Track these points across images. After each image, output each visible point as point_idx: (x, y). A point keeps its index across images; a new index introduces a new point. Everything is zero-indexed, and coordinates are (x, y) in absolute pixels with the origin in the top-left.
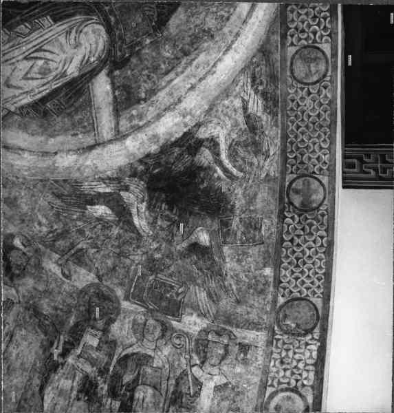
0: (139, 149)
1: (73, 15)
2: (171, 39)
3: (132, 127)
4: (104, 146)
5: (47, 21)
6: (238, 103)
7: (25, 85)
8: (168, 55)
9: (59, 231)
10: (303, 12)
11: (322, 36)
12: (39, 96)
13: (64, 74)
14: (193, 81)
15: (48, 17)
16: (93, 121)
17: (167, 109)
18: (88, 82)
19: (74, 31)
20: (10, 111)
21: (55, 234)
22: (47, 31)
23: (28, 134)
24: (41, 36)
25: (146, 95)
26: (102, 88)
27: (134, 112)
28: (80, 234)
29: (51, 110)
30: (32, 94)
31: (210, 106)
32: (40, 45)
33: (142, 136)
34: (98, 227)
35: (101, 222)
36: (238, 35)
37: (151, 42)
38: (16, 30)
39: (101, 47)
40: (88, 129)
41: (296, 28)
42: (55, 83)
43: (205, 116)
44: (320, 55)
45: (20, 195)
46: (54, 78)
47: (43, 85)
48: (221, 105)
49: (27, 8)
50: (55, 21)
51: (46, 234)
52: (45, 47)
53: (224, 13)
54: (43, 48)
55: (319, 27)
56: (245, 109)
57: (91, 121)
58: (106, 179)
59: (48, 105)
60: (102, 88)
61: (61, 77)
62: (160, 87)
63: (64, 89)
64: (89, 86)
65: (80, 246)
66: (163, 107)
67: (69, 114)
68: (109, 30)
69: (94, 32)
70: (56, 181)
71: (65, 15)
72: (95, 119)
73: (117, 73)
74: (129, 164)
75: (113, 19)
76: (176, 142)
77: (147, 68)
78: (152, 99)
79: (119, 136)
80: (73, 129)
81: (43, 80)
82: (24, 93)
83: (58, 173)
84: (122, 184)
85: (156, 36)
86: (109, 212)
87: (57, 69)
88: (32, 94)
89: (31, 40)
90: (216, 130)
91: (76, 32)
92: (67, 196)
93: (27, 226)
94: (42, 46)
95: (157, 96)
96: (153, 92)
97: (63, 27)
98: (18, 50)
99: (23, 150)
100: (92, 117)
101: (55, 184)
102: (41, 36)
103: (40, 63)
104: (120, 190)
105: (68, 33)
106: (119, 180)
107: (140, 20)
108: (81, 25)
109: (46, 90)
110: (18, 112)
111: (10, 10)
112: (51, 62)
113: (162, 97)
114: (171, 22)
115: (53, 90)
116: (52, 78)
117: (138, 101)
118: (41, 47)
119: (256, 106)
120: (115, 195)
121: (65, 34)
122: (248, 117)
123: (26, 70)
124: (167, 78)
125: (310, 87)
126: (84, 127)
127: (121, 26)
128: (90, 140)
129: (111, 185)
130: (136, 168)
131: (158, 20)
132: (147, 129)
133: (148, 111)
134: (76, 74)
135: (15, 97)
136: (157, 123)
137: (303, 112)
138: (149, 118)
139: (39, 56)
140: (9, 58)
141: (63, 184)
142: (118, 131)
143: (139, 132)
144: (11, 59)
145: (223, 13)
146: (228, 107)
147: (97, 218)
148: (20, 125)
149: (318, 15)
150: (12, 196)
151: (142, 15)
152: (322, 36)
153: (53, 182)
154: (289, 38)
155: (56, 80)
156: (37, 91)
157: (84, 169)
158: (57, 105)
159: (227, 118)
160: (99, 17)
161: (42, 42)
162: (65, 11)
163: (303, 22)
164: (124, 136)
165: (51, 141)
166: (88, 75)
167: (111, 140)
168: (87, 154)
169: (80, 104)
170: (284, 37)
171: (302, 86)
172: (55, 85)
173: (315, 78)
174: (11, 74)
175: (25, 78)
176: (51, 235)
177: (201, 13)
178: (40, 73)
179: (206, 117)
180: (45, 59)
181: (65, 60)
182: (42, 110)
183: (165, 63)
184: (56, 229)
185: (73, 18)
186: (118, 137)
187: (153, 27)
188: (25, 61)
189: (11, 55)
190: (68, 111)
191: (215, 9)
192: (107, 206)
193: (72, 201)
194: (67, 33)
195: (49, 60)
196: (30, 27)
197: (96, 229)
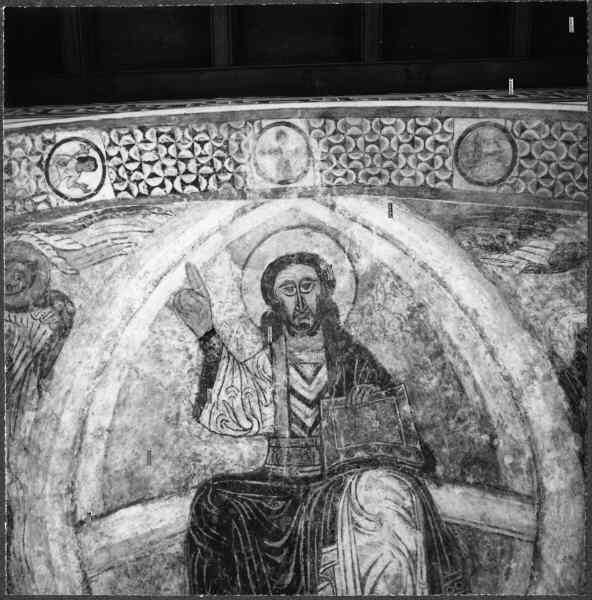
1: (334, 514)
2: (412, 372)
3: (530, 472)
4: (544, 532)
5: (328, 554)
6: (528, 280)
8: (435, 381)
10: (403, 160)
11: (443, 133)
13: (412, 557)
14: (482, 349)
15: (324, 550)
16: (498, 534)
17: (516, 401)
18: (439, 522)
19: (359, 519)
22: (341, 559)
24: (345, 571)
25: (486, 432)
26: (454, 502)
27: (508, 460)
31: (525, 329)
33: (548, 459)
36: (424, 266)
37: (410, 404)
39: (394, 484)
40: (508, 549)
41: (426, 172)
42: (419, 575)
43: (540, 340)
44: (471, 137)
46: (411, 574)
48: (527, 309)
49: (299, 580)
50: (333, 542)
52: (363, 571)
53: (389, 283)
54: (363, 575)
55: (429, 136)
56: (539, 270)
57: (498, 538)
60: (454, 502)
61: (414, 562)
62: (481, 407)
63: (434, 563)
64: (446, 523)
66: (511, 409)
67: (475, 571)
68: (373, 463)
69: (368, 488)
71: (331, 524)
72: (496, 531)
73: (439, 470)
75: (359, 454)
76: (572, 402)
77: (447, 419)
79: (536, 498)
80: (498, 573)
85: (401, 394)
87: (400, 565)
89: (344, 588)
90: (567, 325)
91: (361, 515)
95: (491, 413)
96: (484, 420)
97: (346, 533)
100: (494, 533)
102: (345, 571)
105: (357, 527)
107: (373, 413)
108: (353, 505)
112: (387, 570)
113: (496, 406)
114: (387, 367)
115: (428, 581)
116: (409, 577)
117: (493, 448)
118: (360, 578)
119: (538, 250)
121: (357, 534)
122: (555, 267)
124: (469, 390)
125: (519, 154)
126: (503, 552)
127: (373, 445)
128: (526, 551)
131: (381, 386)
132: (540, 447)
133: (511, 436)
134: (420, 537)
136: (534, 426)
137: (560, 170)
138: (523, 437)
139: (371, 586)
142: (529, 497)
143: (541, 462)
145: (387, 285)
146: (532, 298)
149: (411, 137)
151: (367, 408)
152: (443, 133)
154: (438, 185)
155: (416, 573)
157: (565, 580)
158: (453, 584)
159: (551, 303)
160: (351, 474)
161: (354, 571)
162: (326, 522)
163: (418, 162)
164: (539, 490)
166: (429, 518)
167: (538, 514)
168: (544, 567)
169: (466, 546)
170: (437, 194)
171: (516, 168)
172: (422, 578)
173: (507, 146)
177: (383, 317)
179: (543, 339)
180: (379, 577)
181: (393, 546)
183: (446, 389)
185: (340, 513)
190: (469, 571)
191: (380, 296)
195: (383, 572)
196: (326, 583)
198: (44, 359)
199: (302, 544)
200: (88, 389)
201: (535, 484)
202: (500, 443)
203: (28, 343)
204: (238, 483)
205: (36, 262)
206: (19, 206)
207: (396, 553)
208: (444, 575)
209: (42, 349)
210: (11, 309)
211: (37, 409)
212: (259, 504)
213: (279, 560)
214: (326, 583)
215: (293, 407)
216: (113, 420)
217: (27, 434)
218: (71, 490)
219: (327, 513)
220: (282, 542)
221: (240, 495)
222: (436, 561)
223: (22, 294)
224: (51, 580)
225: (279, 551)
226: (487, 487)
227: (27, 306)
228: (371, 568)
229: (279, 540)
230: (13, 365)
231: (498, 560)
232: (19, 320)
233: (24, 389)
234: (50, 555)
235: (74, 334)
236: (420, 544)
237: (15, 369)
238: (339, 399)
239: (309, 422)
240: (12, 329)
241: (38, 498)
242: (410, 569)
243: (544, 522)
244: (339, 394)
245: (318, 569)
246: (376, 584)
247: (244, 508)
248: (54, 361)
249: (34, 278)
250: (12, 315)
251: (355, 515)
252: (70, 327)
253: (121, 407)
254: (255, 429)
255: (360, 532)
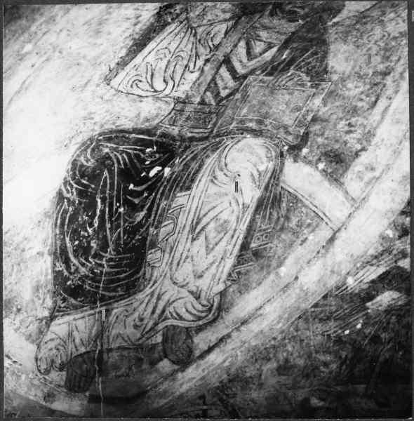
0: (393, 200)
3: (369, 183)
5: (181, 198)
7: (214, 256)
9: (350, 356)
12: (238, 247)
16: (314, 212)
20: (221, 293)
21: (348, 362)
23: (255, 288)
24: (189, 213)
25: (361, 144)
28: (376, 343)
29: (261, 245)
30: (228, 255)
32: (197, 216)
34: (392, 321)
35: (394, 312)
38: (160, 240)
40: (314, 224)
45: (288, 352)
46: (237, 222)
47: (233, 237)
49: (150, 217)
50: (189, 188)
51: (338, 370)
52: (203, 213)
57: (313, 214)
58: (373, 260)
59: (253, 245)
62: (374, 126)
64: (282, 188)
65: (381, 359)
67: (282, 229)
70: (316, 305)
71: (194, 174)
74: (390, 224)
77: (341, 119)
78: (373, 143)
79: (357, 204)
80: (298, 237)
81: (228, 234)
82: (220, 263)
83: (313, 294)
84: (395, 252)
86: (395, 295)
87: (233, 212)
88: (228, 255)
89: (183, 225)
92: (336, 311)
93: (315, 377)
94: (199, 215)
97: (204, 180)
98: (180, 244)
99: (261, 307)
101: (316, 309)
102: (189, 213)
103: (212, 225)
104: (396, 262)
105: (214, 179)
106: (388, 251)
109: (238, 237)
110: (229, 283)
111: (137, 237)
116: (235, 224)
117: (357, 154)
118: (198, 218)
120: (394, 271)
121: (211, 184)
123: (204, 244)
126: (309, 225)
129: (382, 262)
130: (403, 224)
132: (390, 173)
133: (377, 155)
134: (258, 194)
135: (214, 276)
138: (384, 162)
140: (178, 260)
141: (325, 302)
144: (181, 259)
147: (385, 311)
148: (240, 292)
150: (281, 363)
153: (313, 309)
155: (241, 220)
156: (230, 247)
157: (339, 267)
158: (262, 235)
161: (195, 213)
162: (190, 172)
164: (364, 199)
165: (283, 270)
168: (331, 250)
169: (285, 209)
174: (194, 265)
175: (209, 250)
176: (344, 367)
178: (219, 233)
182: (251, 255)
183: (362, 100)
184: (346, 356)
185: (205, 167)
186: (356, 206)
187: (312, 87)
188: (195, 242)
189: (177, 255)
190: (278, 228)
192: (391, 290)
193: (346, 311)
194: (212, 181)
195: (217, 215)
196: (171, 221)
197: (391, 326)
199: (162, 188)
201: (365, 194)
202: (364, 158)
204: (123, 136)
207: (234, 204)
208: (260, 227)
212: (135, 155)
213: (136, 201)
214: (171, 221)
215: (218, 77)
219: (194, 166)
220: (144, 187)
221: (121, 148)
222: (259, 214)
225: (139, 194)
226: (329, 176)
228: (209, 211)
229: (143, 184)
231: (303, 228)
236: (255, 200)
238: (266, 78)
239: (224, 93)
242: (238, 218)
243: (351, 223)
244: (270, 74)
245: (168, 210)
246: (208, 224)
247: (120, 158)
251: (217, 170)
254: (167, 92)
255: (214, 183)
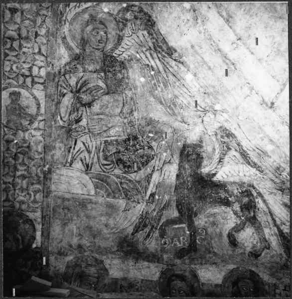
198: (160, 47)
200: (200, 33)
203: (144, 49)
205: (91, 16)
206: (45, 12)
209: (153, 43)
210: (115, 48)
211: (188, 70)
216: (234, 31)
217: (198, 86)
218: (252, 89)
223: (109, 36)
224: (279, 151)
227: (119, 36)
230: (152, 66)
232: (126, 47)
233: (170, 69)
234: (268, 136)
235: (156, 18)
237: (155, 66)
240: (129, 53)
241: (237, 108)
248: (164, 41)
249: (101, 23)
250: (120, 49)
252: (150, 17)
253: (230, 19)
